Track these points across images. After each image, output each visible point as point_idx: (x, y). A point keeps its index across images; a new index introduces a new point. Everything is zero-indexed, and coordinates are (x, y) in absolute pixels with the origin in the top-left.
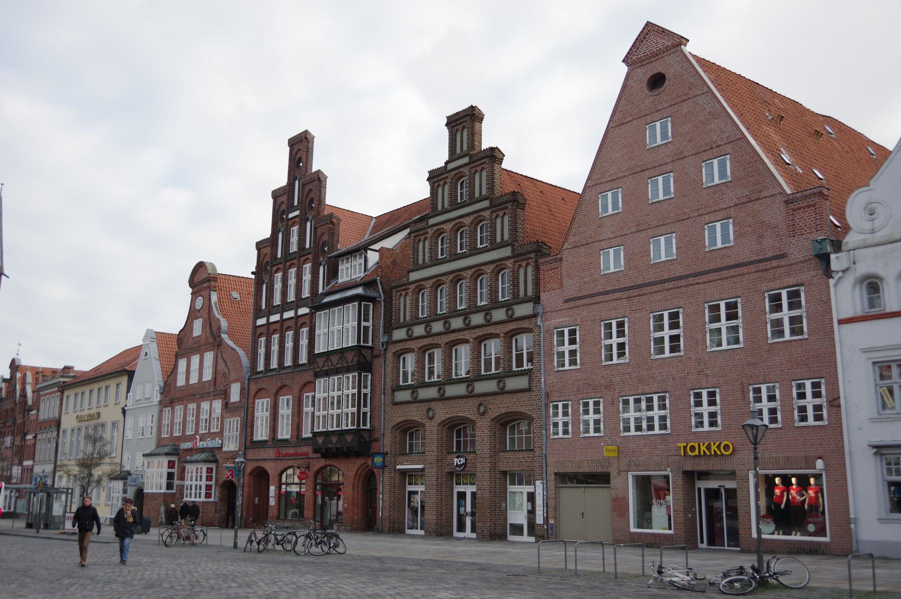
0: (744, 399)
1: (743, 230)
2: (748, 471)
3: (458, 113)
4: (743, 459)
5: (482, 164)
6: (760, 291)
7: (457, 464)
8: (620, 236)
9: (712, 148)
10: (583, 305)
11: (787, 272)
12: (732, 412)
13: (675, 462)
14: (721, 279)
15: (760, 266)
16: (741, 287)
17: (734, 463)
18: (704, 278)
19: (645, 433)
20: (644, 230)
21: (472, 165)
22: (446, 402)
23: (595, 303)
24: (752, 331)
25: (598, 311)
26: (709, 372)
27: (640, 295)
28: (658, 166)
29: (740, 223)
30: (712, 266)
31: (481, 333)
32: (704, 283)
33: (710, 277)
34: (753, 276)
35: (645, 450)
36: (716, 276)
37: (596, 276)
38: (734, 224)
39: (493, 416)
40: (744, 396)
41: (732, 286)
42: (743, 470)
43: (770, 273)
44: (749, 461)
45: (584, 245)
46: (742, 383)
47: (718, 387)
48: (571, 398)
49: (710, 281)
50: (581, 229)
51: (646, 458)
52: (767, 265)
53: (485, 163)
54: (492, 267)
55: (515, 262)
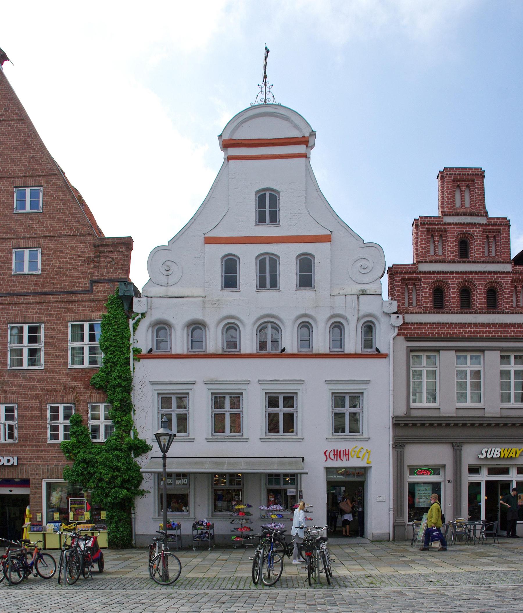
0: (41, 416)
1: (51, 261)
2: (42, 479)
4: (38, 469)
6: (63, 320)
9: (25, 177)
11: (91, 307)
12: (30, 427)
14: (26, 304)
15: (66, 298)
16: (46, 314)
17: (28, 472)
18: (9, 300)
24: (53, 355)
26: (8, 389)
29: (48, 254)
30: (18, 289)
32: (9, 304)
33: (15, 299)
34: (58, 306)
36: (22, 299)
38: (42, 254)
40: (42, 414)
41: (37, 312)
42: (37, 479)
43: (75, 305)
44: (43, 471)
46: (40, 402)
47: (17, 404)
49: (15, 304)
52: (72, 297)
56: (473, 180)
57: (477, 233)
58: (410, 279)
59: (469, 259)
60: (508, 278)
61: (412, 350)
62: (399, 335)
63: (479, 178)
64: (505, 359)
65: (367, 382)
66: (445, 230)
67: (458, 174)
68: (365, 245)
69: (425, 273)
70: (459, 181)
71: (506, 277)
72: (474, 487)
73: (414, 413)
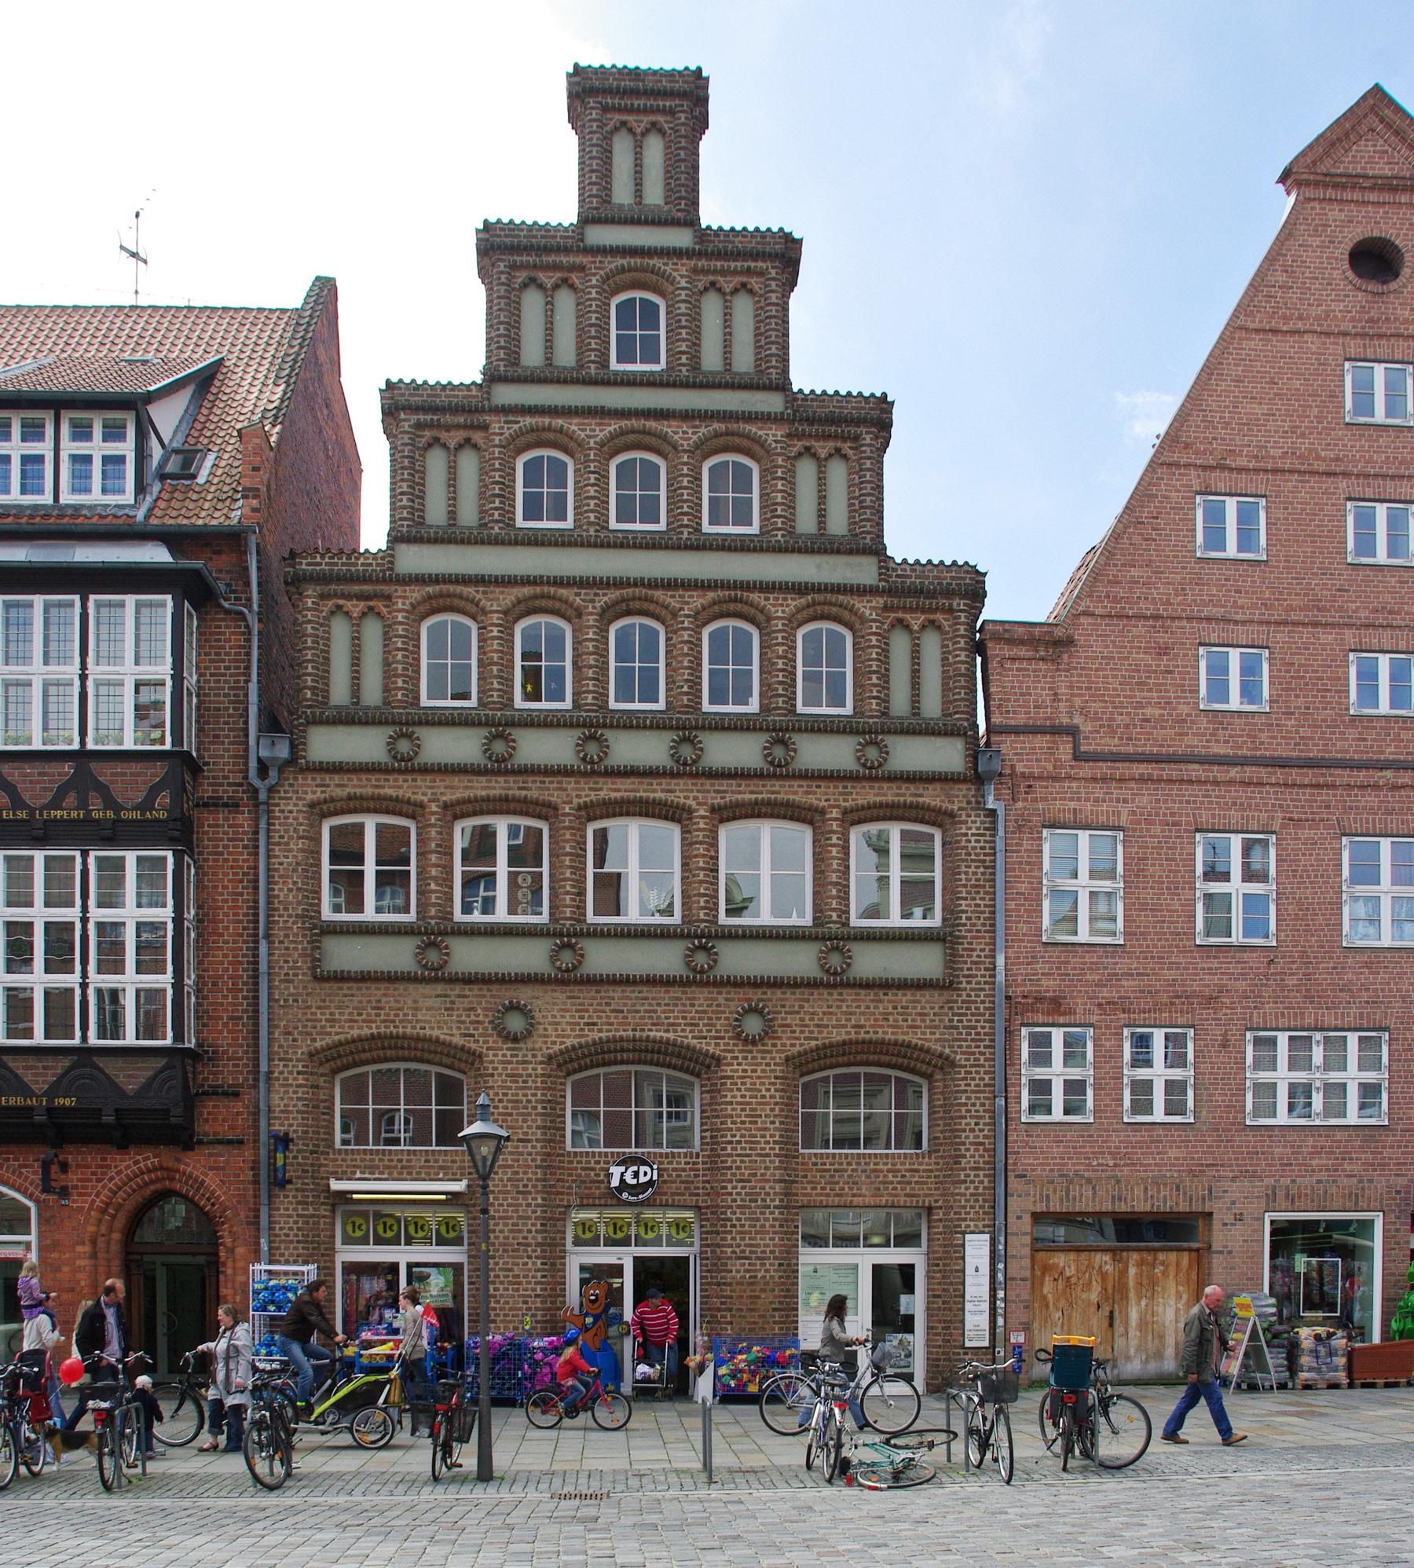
3: (636, 74)
5: (749, 272)
7: (622, 1180)
8: (1261, 623)
10: (1142, 780)
13: (1398, 1192)
19: (1318, 1122)
20: (1333, 625)
21: (702, 263)
22: (588, 994)
23: (1181, 781)
25: (1188, 802)
27: (1318, 786)
28: (1376, 476)
31: (747, 797)
35: (1314, 1162)
37: (1184, 710)
39: (798, 1048)
45: (1146, 618)
48: (1094, 1019)
50: (1134, 572)
51: (1319, 1181)
53: (761, 273)
54: (793, 603)
55: (886, 608)
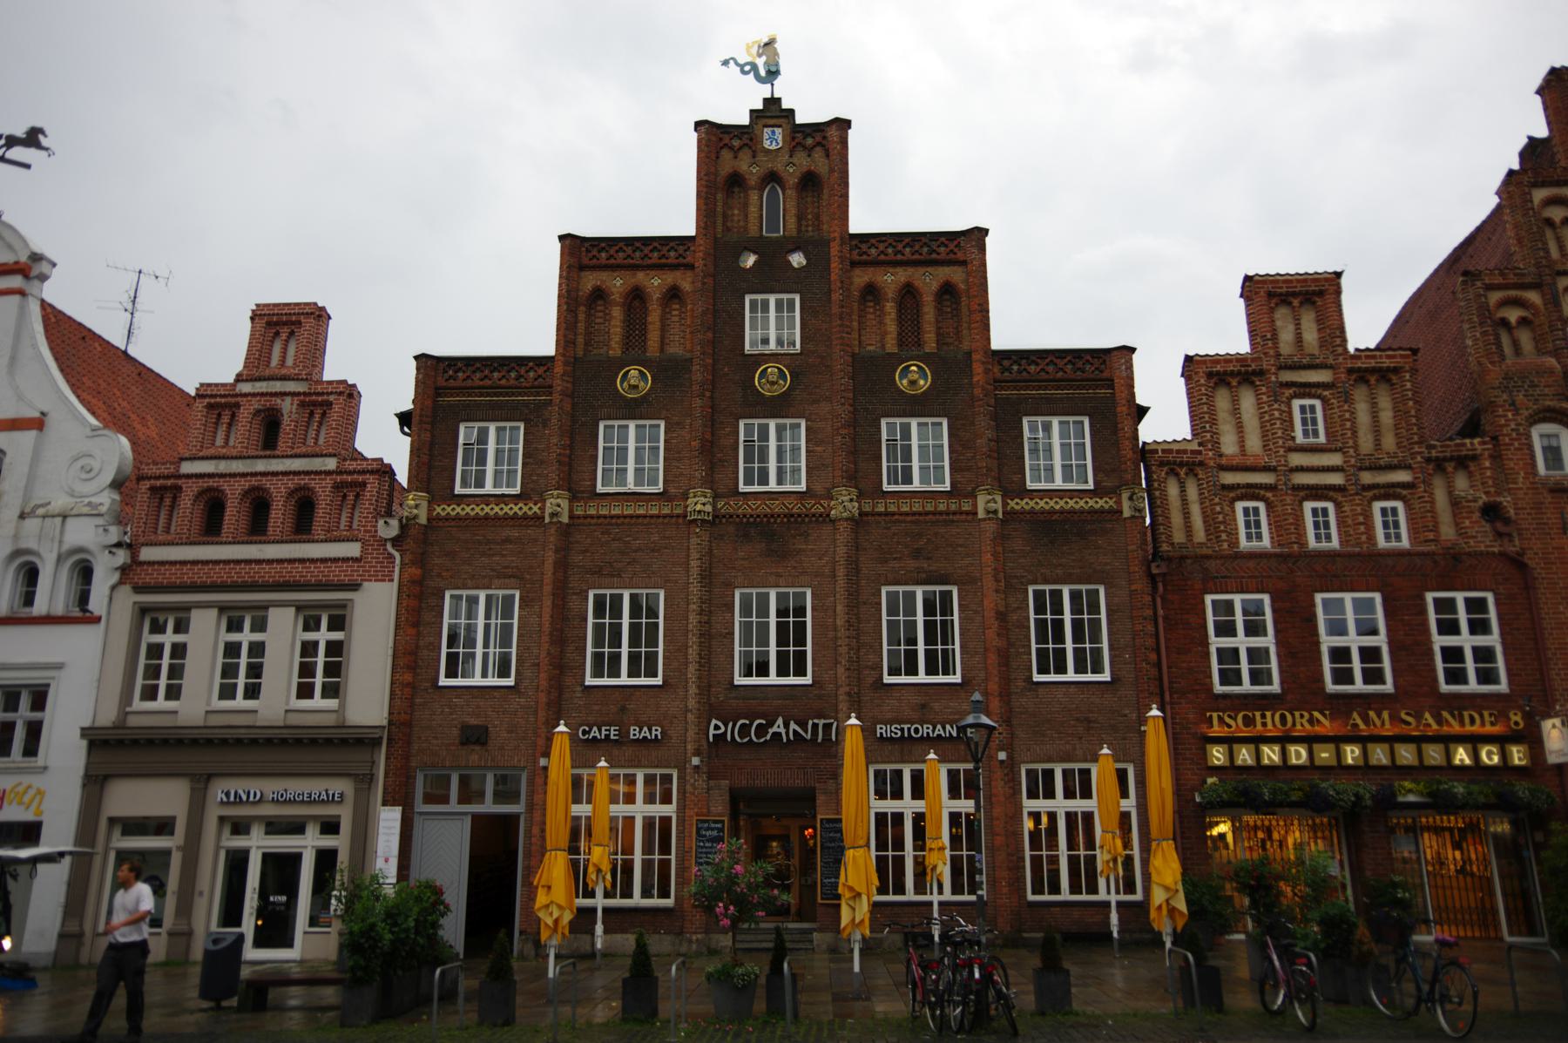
56: (299, 323)
57: (287, 406)
58: (164, 488)
59: (277, 453)
60: (329, 481)
61: (143, 611)
62: (125, 583)
63: (310, 318)
64: (311, 624)
65: (59, 667)
66: (237, 405)
67: (273, 315)
68: (95, 433)
69: (189, 476)
70: (277, 324)
71: (325, 479)
72: (237, 863)
73: (133, 721)
